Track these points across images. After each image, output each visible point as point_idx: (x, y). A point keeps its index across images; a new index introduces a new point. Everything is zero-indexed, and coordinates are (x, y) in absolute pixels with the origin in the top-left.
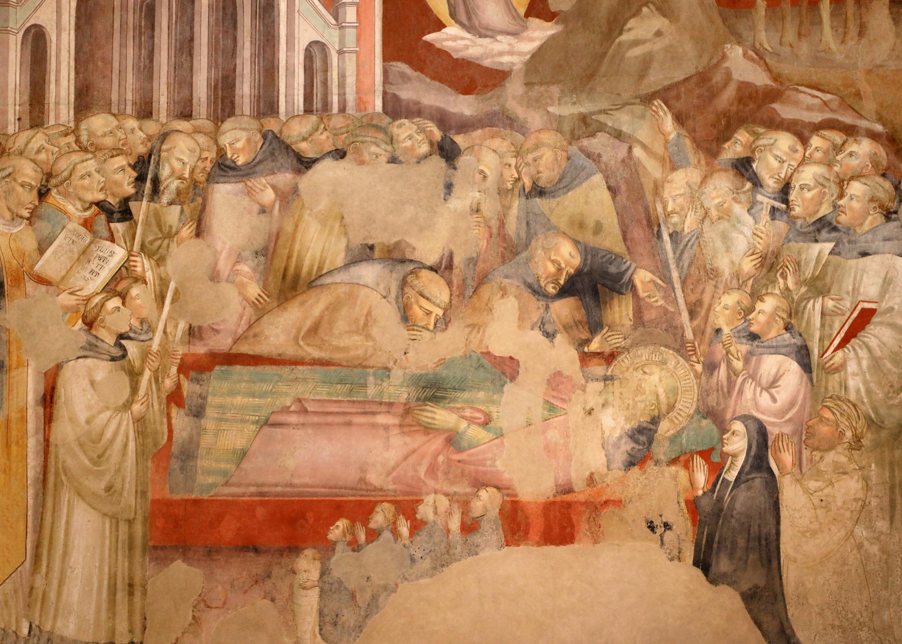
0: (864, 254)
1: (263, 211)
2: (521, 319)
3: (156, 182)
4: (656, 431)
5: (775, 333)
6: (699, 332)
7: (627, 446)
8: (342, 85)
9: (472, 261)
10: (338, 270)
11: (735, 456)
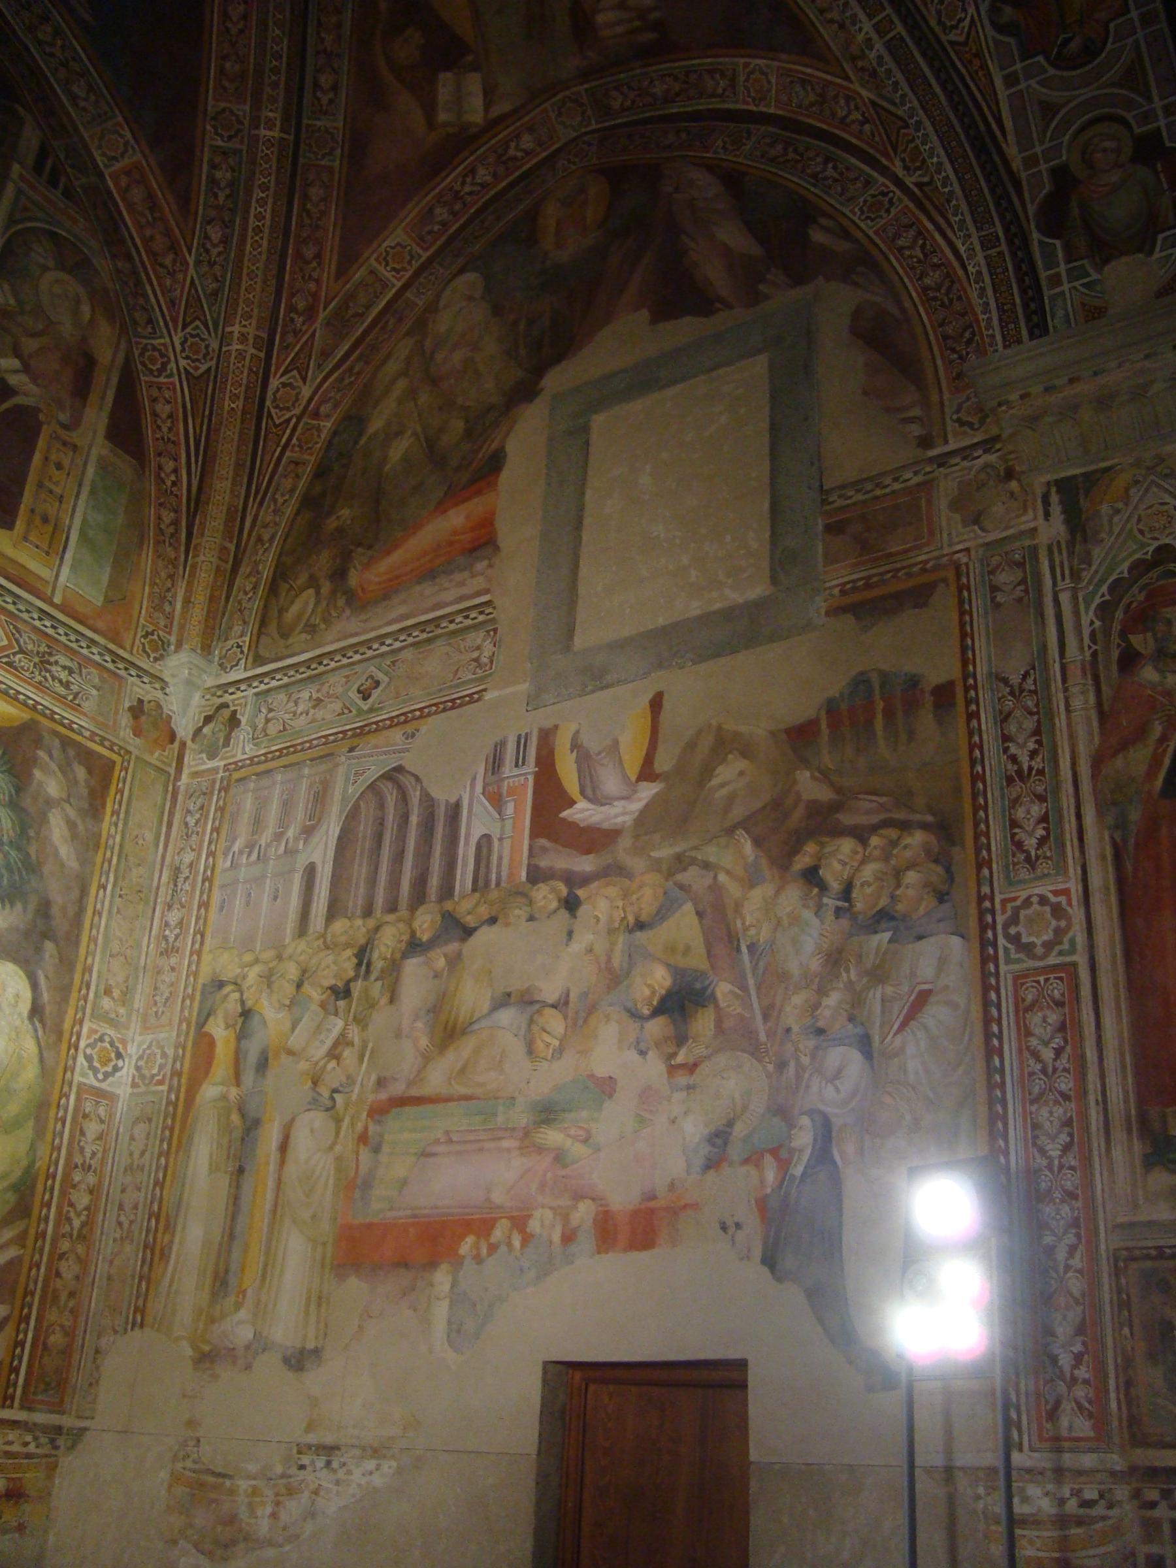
0: (920, 938)
1: (437, 976)
3: (369, 965)
4: (730, 1134)
6: (771, 1034)
7: (705, 1150)
8: (499, 865)
9: (584, 995)
10: (484, 1017)
11: (801, 1151)
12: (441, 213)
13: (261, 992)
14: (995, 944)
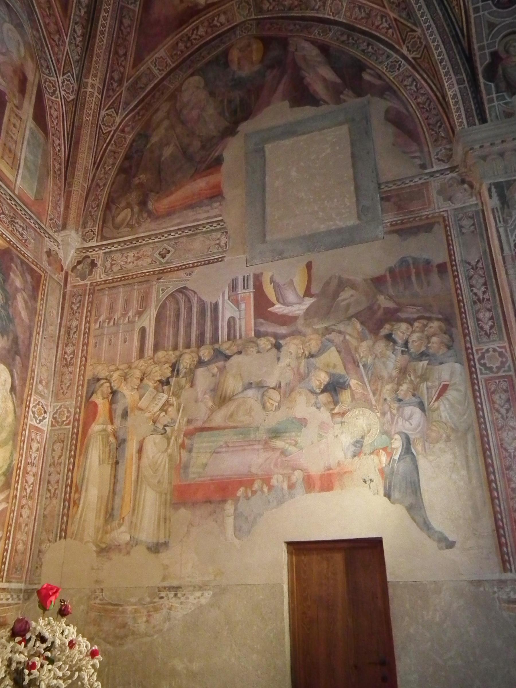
0: (441, 363)
2: (307, 403)
3: (178, 371)
5: (409, 398)
7: (352, 448)
8: (240, 330)
9: (288, 384)
10: (240, 393)
11: (397, 449)
12: (181, 46)
13: (121, 383)
14: (475, 367)
